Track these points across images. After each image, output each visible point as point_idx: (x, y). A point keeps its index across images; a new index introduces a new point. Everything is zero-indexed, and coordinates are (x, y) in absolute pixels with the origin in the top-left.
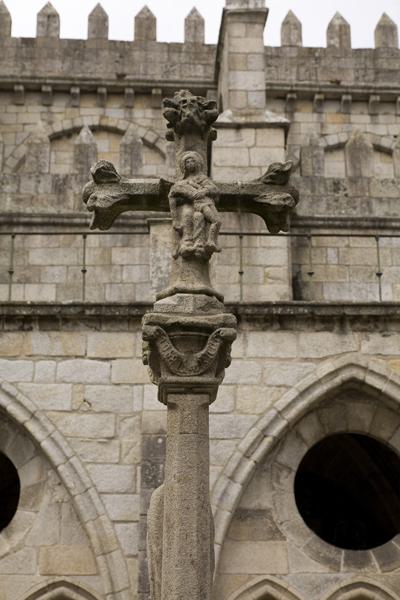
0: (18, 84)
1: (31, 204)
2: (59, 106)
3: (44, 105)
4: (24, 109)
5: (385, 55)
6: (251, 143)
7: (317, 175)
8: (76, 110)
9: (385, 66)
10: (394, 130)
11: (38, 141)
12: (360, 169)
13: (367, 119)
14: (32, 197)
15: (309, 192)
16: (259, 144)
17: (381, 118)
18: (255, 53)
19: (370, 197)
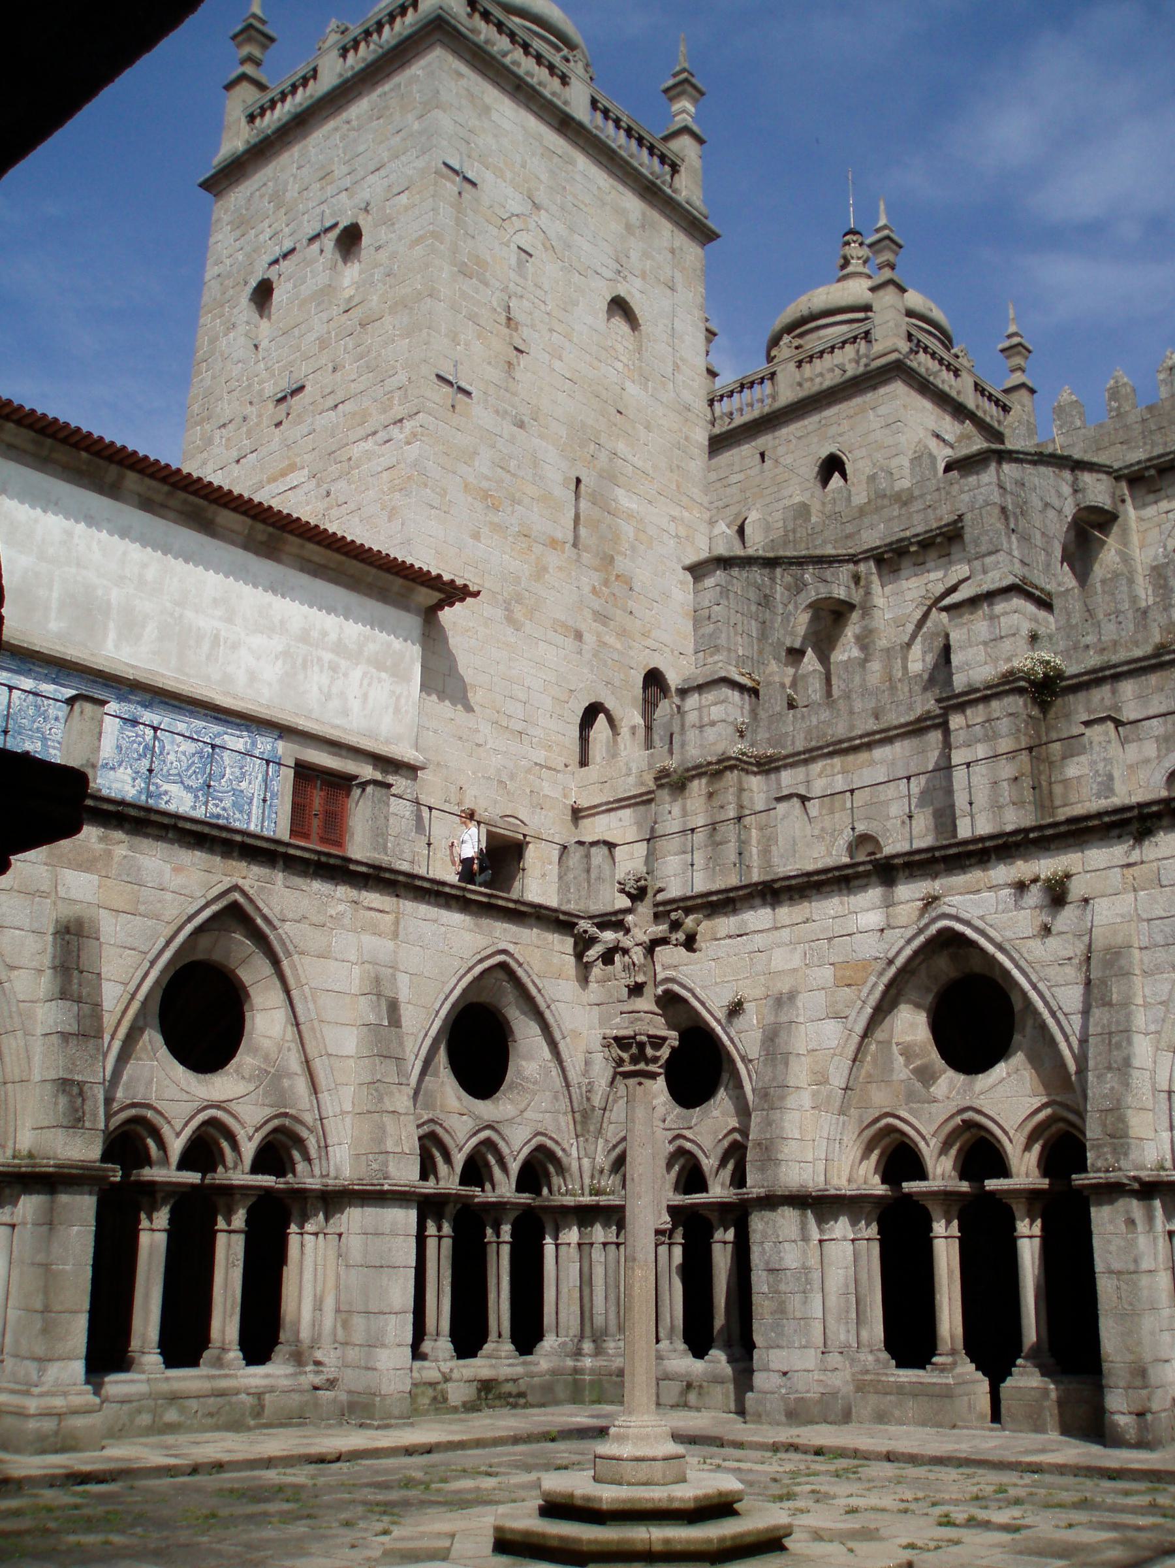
0: (1147, 468)
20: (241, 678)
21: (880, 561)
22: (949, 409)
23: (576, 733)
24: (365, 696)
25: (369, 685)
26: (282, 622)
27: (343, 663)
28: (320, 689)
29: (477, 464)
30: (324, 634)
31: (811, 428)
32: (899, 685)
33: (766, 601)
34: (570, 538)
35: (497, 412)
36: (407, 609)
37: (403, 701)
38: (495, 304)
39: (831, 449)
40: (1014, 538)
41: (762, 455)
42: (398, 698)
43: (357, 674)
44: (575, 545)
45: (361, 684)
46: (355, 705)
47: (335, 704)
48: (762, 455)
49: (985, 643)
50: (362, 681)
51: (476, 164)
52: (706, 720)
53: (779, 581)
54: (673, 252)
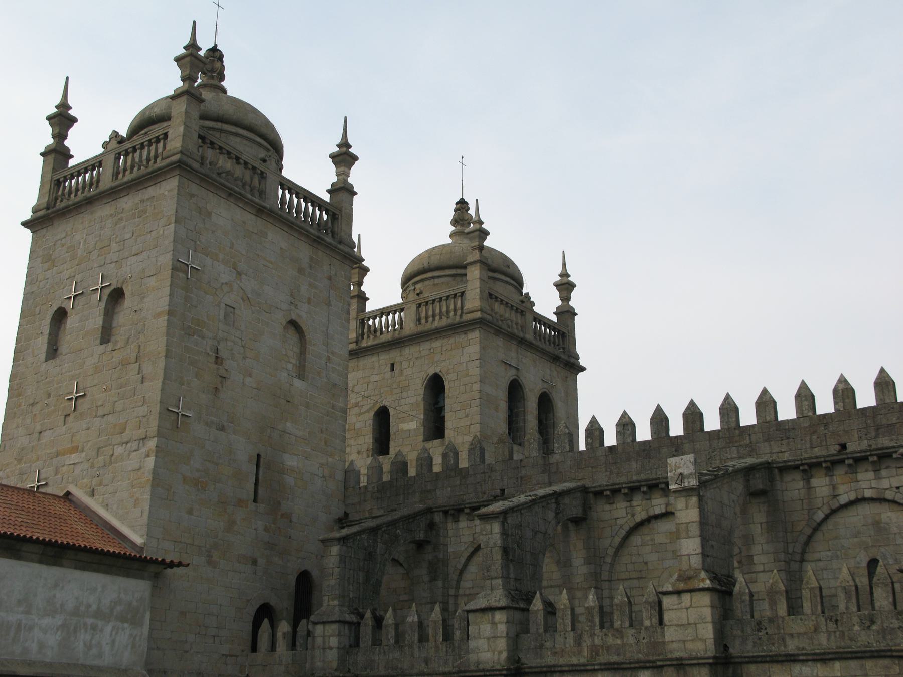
1: (562, 656)
2: (638, 501)
3: (628, 501)
4: (614, 506)
5: (883, 412)
6: (688, 604)
7: (744, 617)
8: (649, 501)
9: (884, 422)
10: (895, 482)
11: (563, 607)
12: (776, 611)
13: (871, 475)
14: (563, 651)
15: (739, 633)
16: (693, 605)
17: (884, 473)
18: (693, 522)
19: (784, 634)
20: (34, 647)
21: (446, 513)
22: (515, 342)
23: (249, 628)
24: (113, 642)
25: (117, 634)
26: (62, 605)
27: (100, 623)
28: (85, 644)
29: (192, 462)
30: (89, 606)
31: (424, 353)
32: (441, 646)
33: (370, 556)
34: (252, 497)
35: (207, 424)
36: (143, 578)
37: (138, 639)
38: (208, 349)
39: (438, 371)
40: (511, 566)
41: (393, 365)
42: (135, 638)
43: (109, 628)
44: (255, 501)
45: (111, 635)
46: (107, 649)
47: (94, 651)
48: (393, 365)
49: (488, 639)
50: (112, 631)
51: (200, 254)
52: (327, 645)
53: (379, 540)
54: (330, 278)
